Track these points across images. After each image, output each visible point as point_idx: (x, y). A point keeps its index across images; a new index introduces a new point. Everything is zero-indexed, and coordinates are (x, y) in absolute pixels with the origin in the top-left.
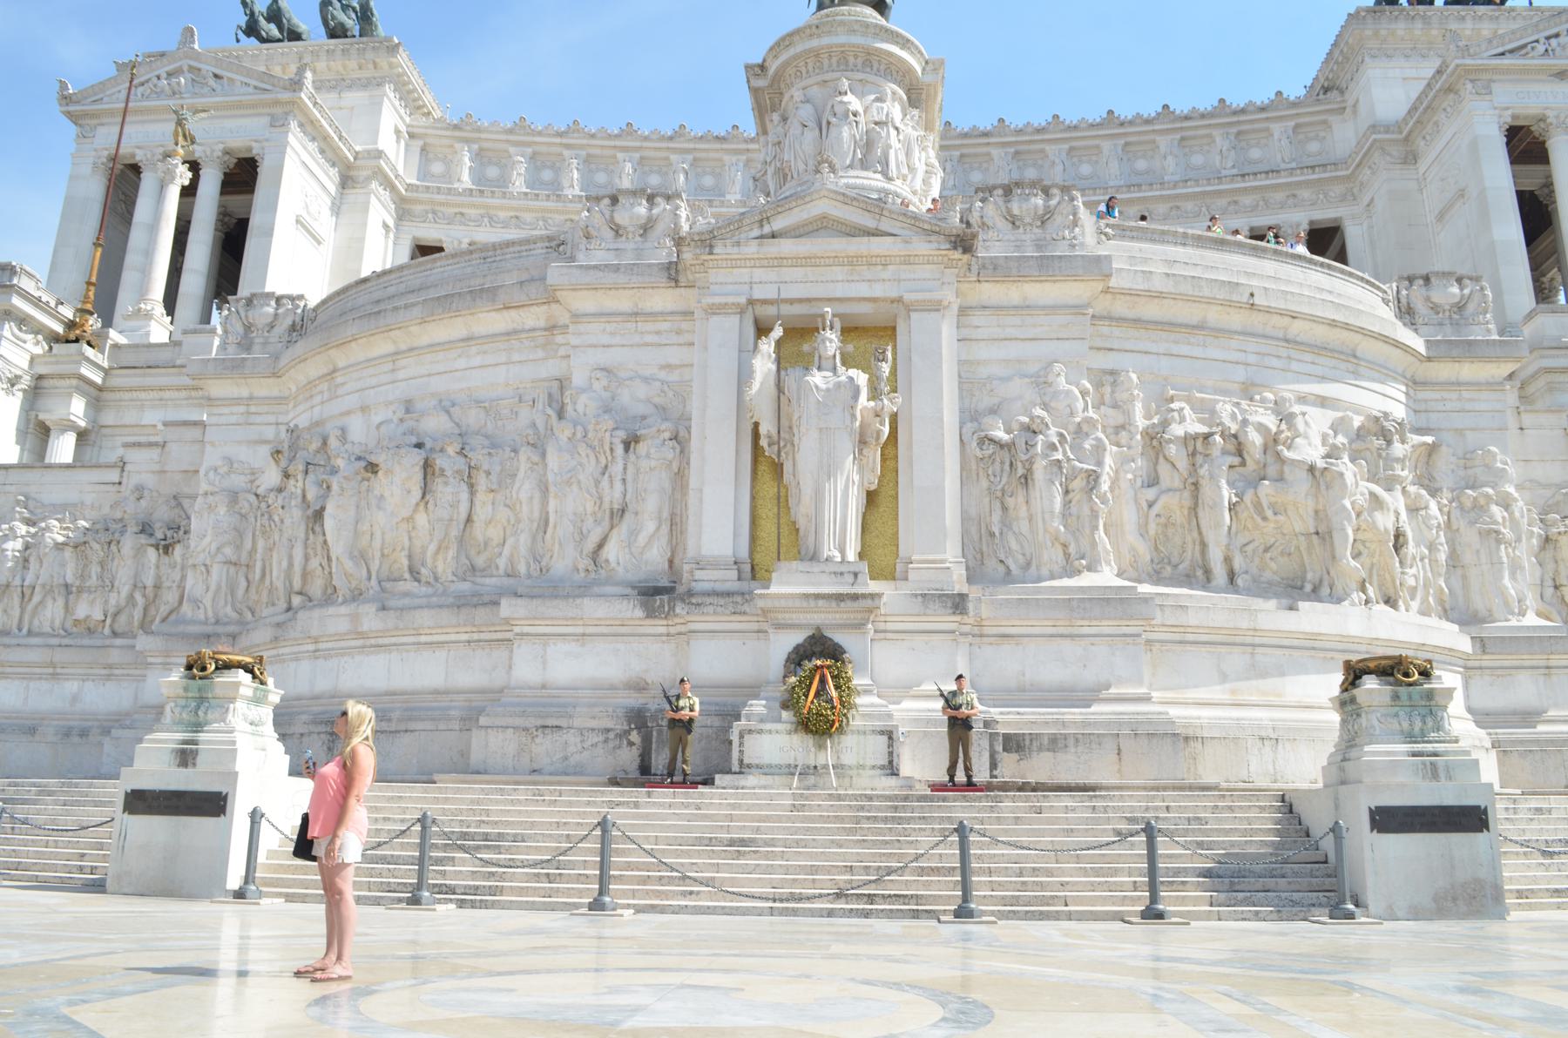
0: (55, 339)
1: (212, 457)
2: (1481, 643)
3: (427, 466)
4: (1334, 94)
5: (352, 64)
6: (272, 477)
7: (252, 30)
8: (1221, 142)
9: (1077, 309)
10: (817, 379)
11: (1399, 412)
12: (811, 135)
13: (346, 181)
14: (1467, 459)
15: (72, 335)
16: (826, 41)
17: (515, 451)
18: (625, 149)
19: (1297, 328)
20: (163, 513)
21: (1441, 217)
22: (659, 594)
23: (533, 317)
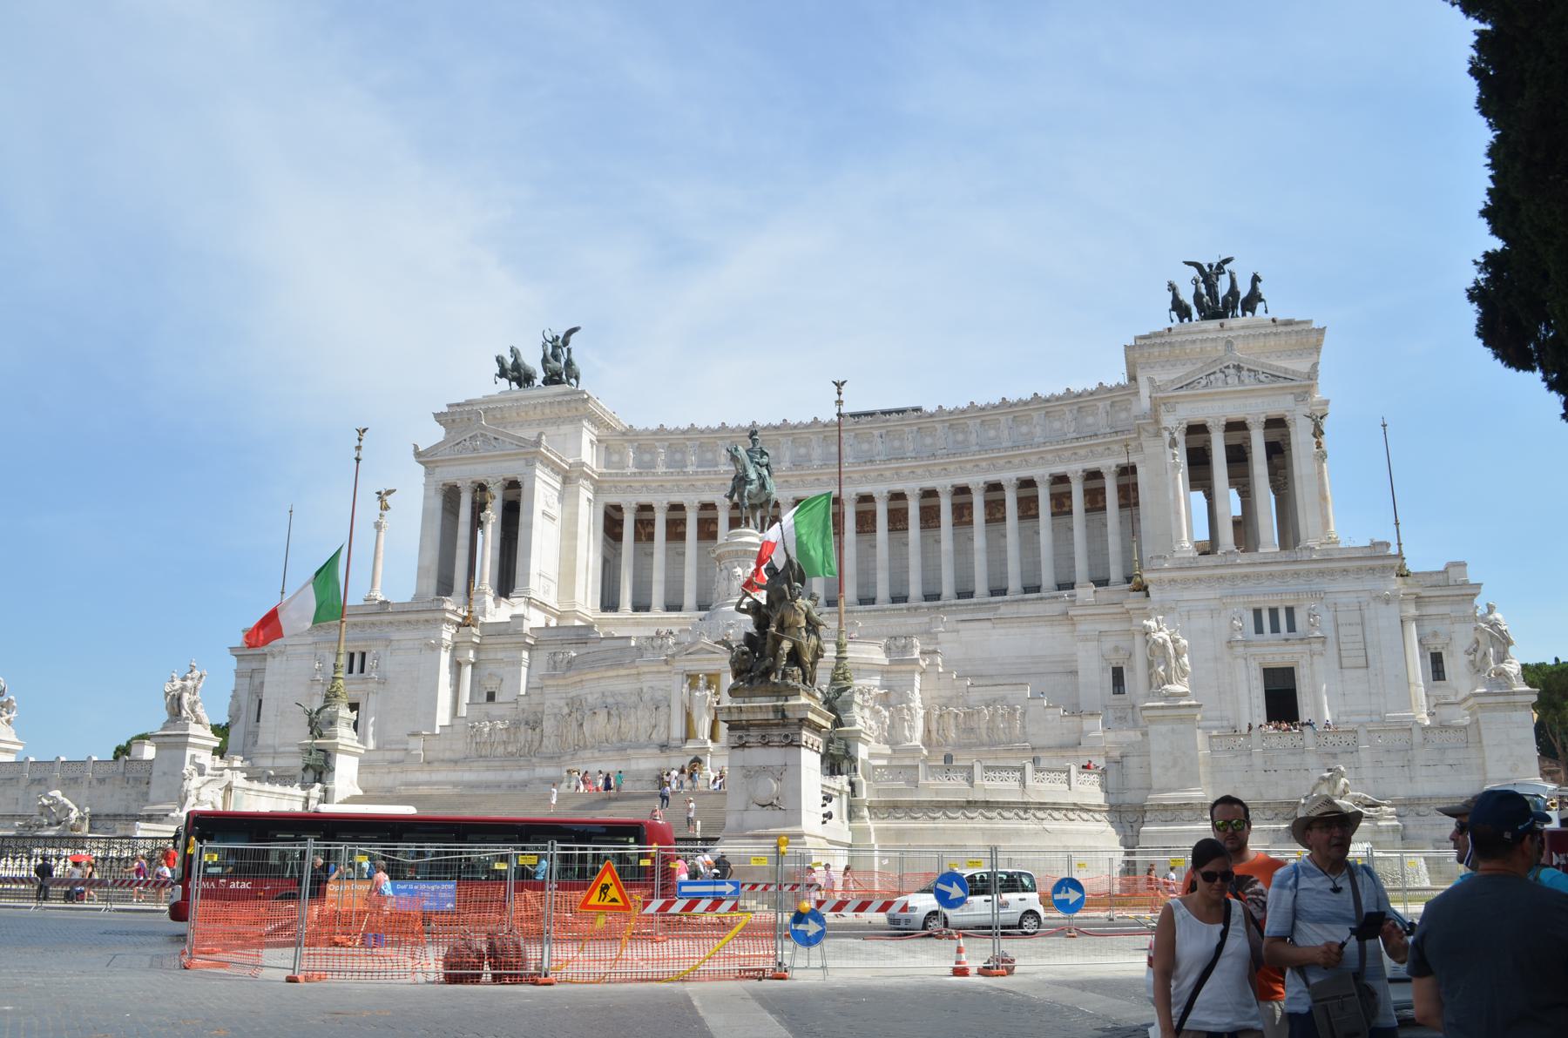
0: (459, 625)
1: (548, 703)
2: (894, 751)
6: (566, 710)
7: (503, 373)
8: (1069, 416)
11: (878, 683)
13: (567, 479)
15: (466, 623)
18: (722, 438)
20: (532, 718)
22: (664, 747)
23: (634, 671)
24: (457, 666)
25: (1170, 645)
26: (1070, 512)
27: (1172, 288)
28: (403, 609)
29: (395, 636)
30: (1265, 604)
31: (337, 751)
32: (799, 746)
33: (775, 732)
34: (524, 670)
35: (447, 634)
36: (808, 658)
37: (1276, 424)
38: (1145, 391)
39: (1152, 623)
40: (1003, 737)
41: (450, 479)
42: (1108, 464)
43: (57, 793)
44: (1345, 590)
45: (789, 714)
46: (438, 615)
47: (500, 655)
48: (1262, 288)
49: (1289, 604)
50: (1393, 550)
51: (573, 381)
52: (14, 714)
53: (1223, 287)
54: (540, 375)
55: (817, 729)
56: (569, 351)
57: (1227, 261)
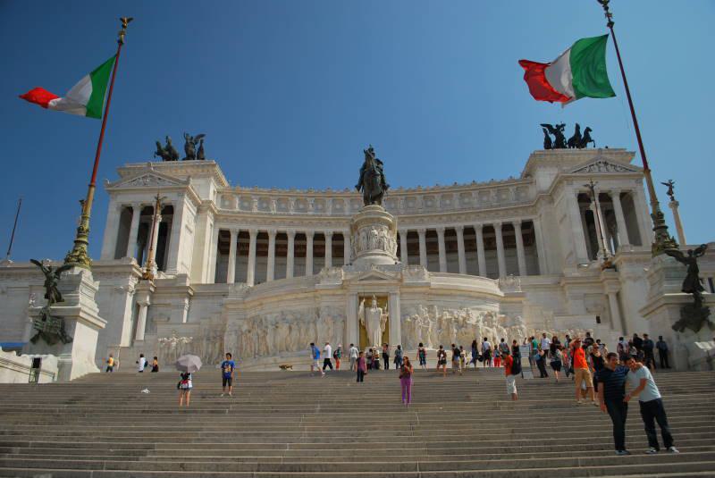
0: (140, 278)
1: (230, 322)
3: (290, 328)
4: (528, 178)
5: (200, 170)
6: (245, 328)
8: (493, 193)
10: (372, 310)
11: (497, 310)
12: (365, 241)
13: (199, 211)
14: (513, 320)
16: (369, 216)
17: (309, 323)
19: (472, 294)
20: (212, 334)
21: (561, 221)
31: (76, 318)
34: (186, 312)
42: (517, 220)
46: (127, 270)
47: (168, 301)
48: (591, 134)
49: (711, 276)
53: (568, 134)
54: (182, 154)
56: (202, 142)
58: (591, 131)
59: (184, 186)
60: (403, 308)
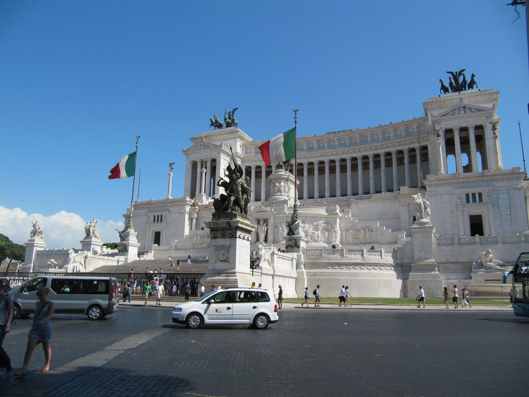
0: (192, 206)
7: (212, 125)
9: (284, 217)
15: (194, 205)
24: (191, 220)
25: (422, 204)
26: (404, 164)
27: (441, 81)
28: (173, 201)
29: (171, 209)
30: (470, 191)
31: (129, 245)
32: (236, 237)
33: (227, 232)
35: (188, 208)
36: (243, 203)
37: (479, 128)
38: (430, 119)
39: (416, 196)
40: (369, 241)
41: (194, 160)
43: (53, 260)
44: (501, 185)
45: (232, 225)
48: (475, 79)
50: (522, 170)
51: (235, 126)
52: (43, 235)
55: (249, 232)
57: (463, 71)
58: (474, 76)
59: (219, 148)
60: (275, 224)
